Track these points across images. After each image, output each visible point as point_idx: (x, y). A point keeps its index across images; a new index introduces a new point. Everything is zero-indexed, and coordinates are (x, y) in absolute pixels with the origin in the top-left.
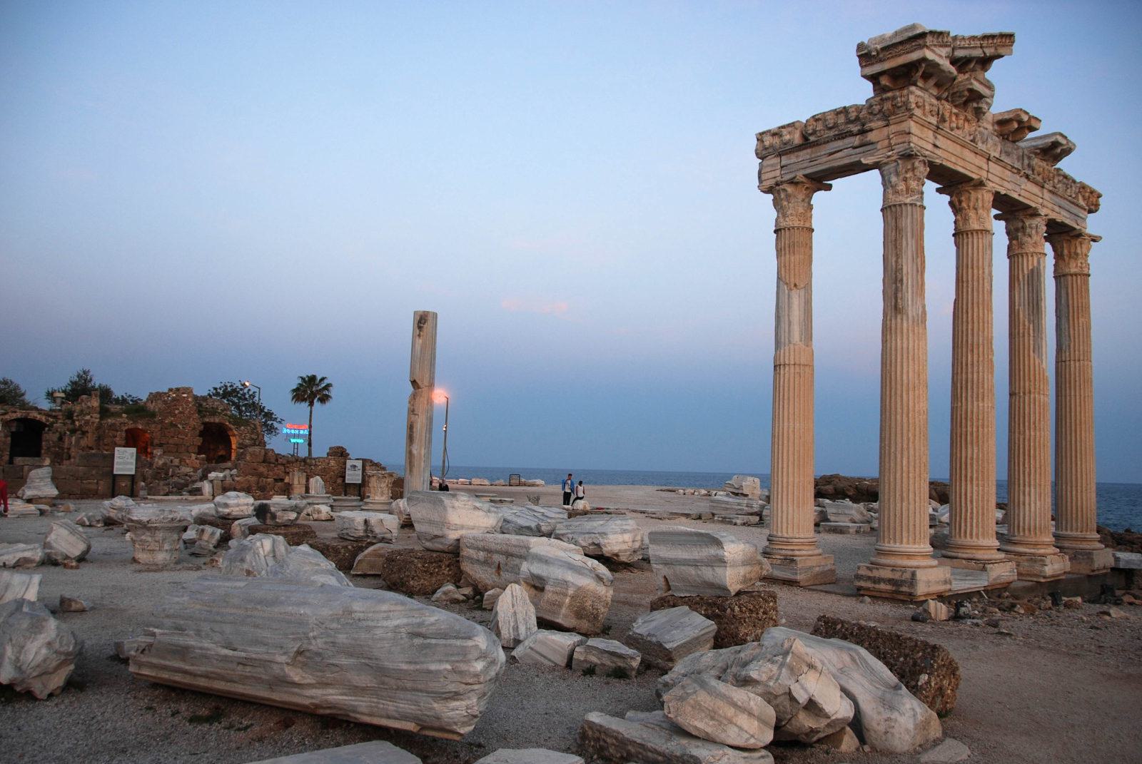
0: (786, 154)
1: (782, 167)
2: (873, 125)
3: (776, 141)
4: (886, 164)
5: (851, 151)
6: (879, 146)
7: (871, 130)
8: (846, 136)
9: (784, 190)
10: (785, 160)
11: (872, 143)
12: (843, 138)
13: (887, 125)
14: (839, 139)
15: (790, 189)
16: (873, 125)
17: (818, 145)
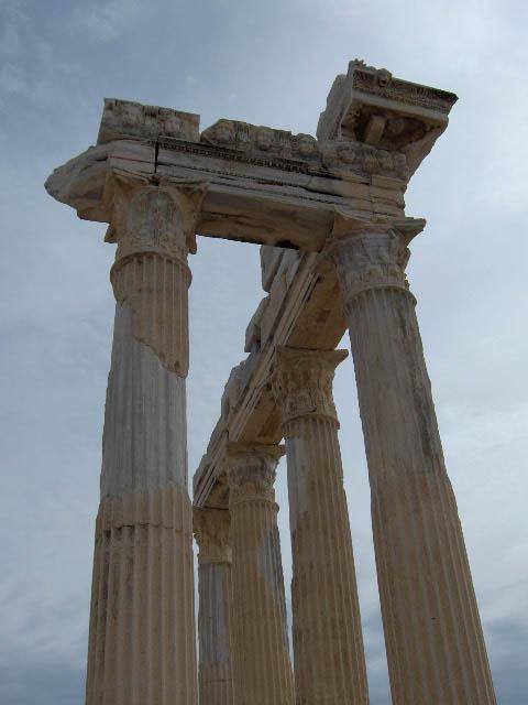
0: (173, 148)
1: (157, 164)
2: (345, 173)
3: (149, 122)
4: (371, 230)
5: (303, 192)
6: (353, 203)
7: (340, 179)
8: (295, 168)
9: (166, 195)
10: (164, 155)
11: (341, 196)
12: (289, 170)
13: (367, 184)
14: (280, 167)
15: (179, 199)
16: (345, 173)
17: (239, 159)
